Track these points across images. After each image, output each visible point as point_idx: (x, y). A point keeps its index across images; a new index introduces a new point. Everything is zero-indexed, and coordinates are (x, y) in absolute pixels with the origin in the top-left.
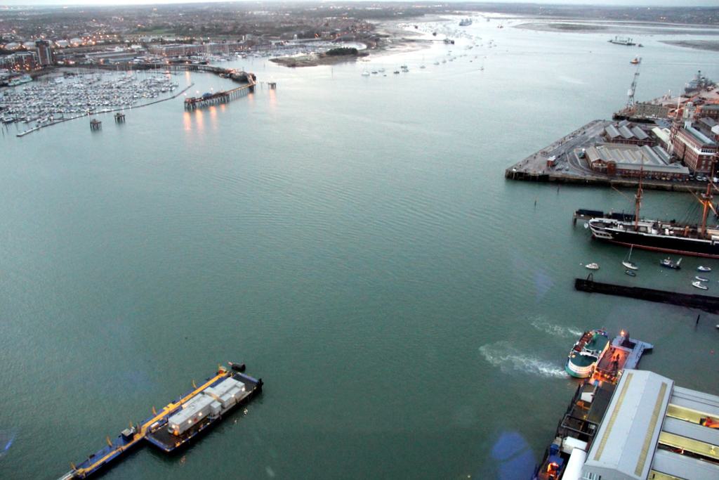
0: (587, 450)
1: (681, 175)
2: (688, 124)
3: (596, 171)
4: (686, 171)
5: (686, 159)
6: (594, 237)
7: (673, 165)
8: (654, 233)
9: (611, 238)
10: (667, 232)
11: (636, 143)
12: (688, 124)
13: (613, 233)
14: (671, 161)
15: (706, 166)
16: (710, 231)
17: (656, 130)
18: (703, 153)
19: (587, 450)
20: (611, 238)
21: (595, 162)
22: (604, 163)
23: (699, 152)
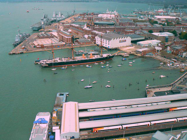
0: (60, 128)
1: (63, 45)
2: (62, 30)
3: (38, 48)
4: (64, 43)
5: (63, 40)
6: (42, 66)
7: (60, 42)
8: (59, 61)
9: (48, 65)
10: (63, 60)
11: (48, 38)
12: (62, 30)
13: (48, 64)
14: (59, 41)
15: (69, 41)
16: (75, 57)
17: (53, 33)
18: (68, 37)
19: (60, 128)
20: (48, 65)
21: (37, 45)
22: (40, 45)
23: (67, 37)
